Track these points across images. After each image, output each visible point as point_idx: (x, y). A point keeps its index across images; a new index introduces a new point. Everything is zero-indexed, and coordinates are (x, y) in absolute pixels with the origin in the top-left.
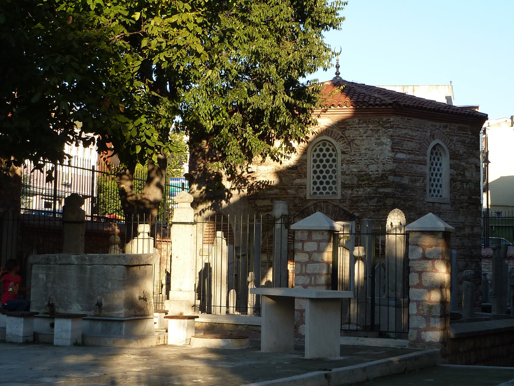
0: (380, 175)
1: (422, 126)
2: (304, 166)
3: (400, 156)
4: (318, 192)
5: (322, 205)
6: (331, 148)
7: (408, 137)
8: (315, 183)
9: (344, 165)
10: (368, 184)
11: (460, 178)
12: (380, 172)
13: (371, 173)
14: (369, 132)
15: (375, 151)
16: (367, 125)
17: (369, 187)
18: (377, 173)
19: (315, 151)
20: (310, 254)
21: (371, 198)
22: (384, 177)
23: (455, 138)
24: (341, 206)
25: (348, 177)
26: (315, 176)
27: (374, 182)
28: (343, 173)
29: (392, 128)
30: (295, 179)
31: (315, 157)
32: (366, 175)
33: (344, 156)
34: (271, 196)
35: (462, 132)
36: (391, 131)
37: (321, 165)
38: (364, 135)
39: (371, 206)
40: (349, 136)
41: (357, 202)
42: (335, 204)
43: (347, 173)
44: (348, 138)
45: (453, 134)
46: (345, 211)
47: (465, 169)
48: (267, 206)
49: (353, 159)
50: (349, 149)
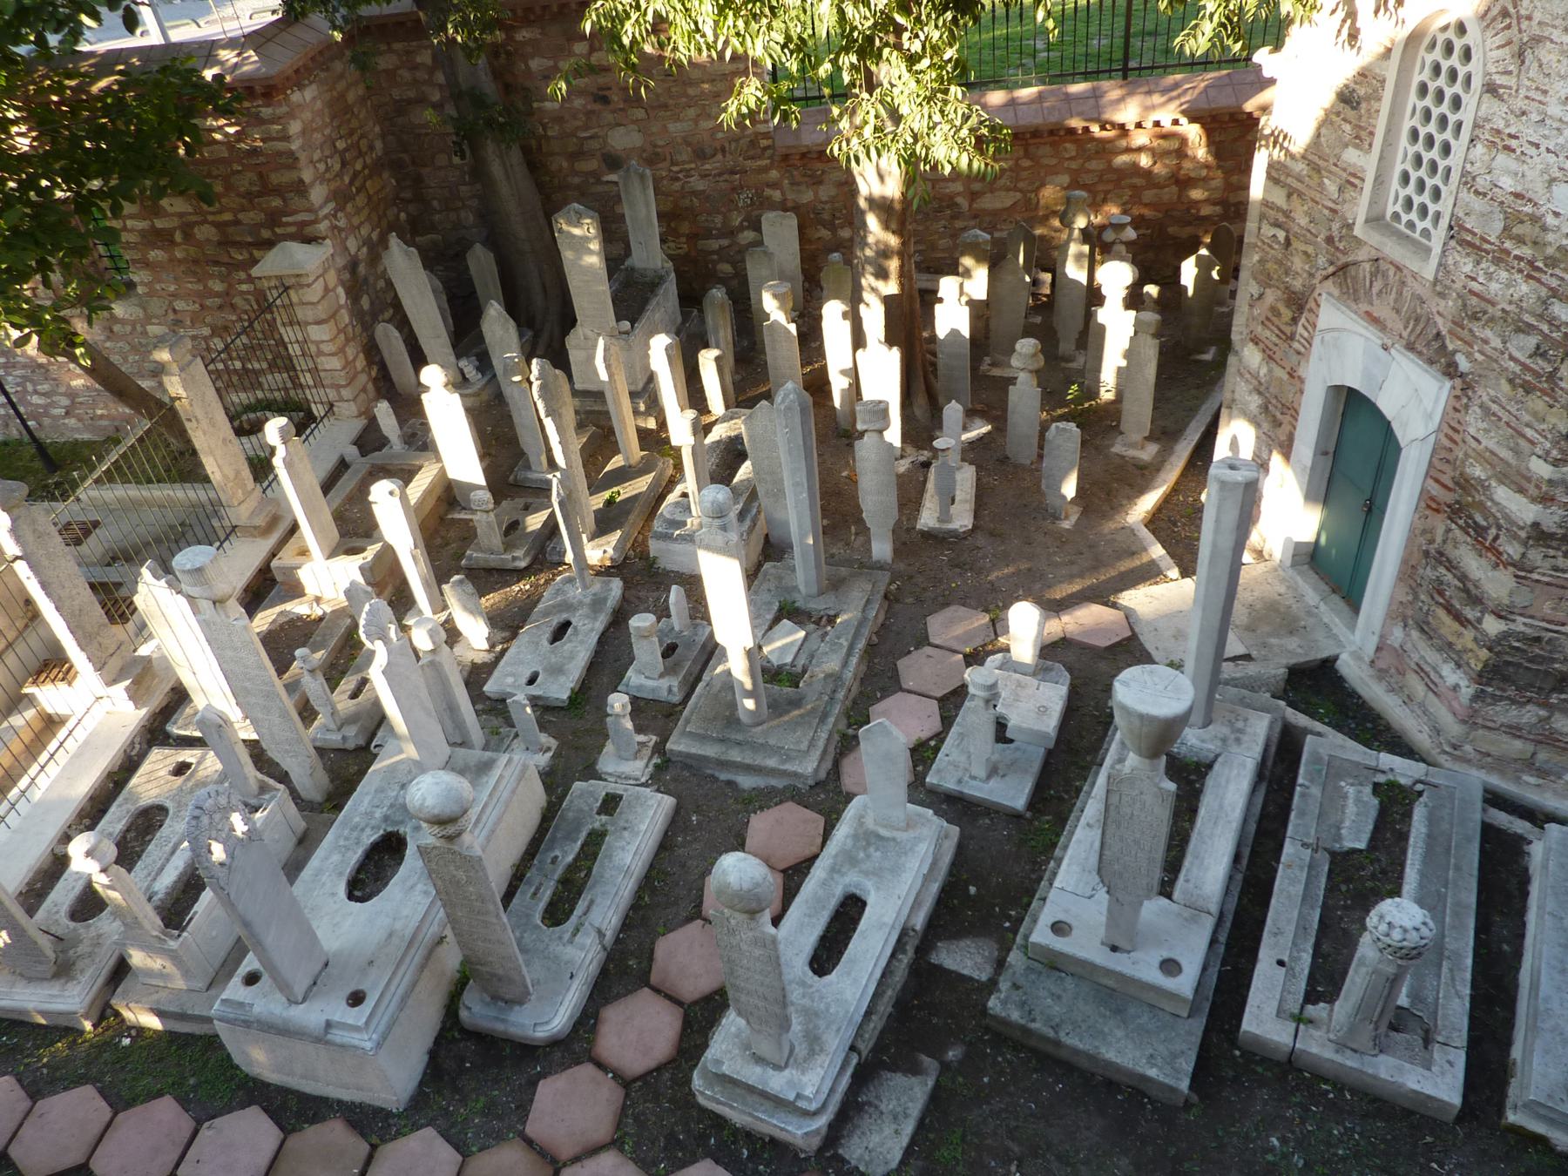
9: (1480, 149)
10: (1531, 263)
13: (1550, 220)
17: (1529, 277)
21: (1525, 329)
25: (1478, 204)
28: (1468, 180)
39: (1512, 358)
41: (1475, 317)
43: (1481, 183)
49: (1512, 130)
50: (1512, 82)
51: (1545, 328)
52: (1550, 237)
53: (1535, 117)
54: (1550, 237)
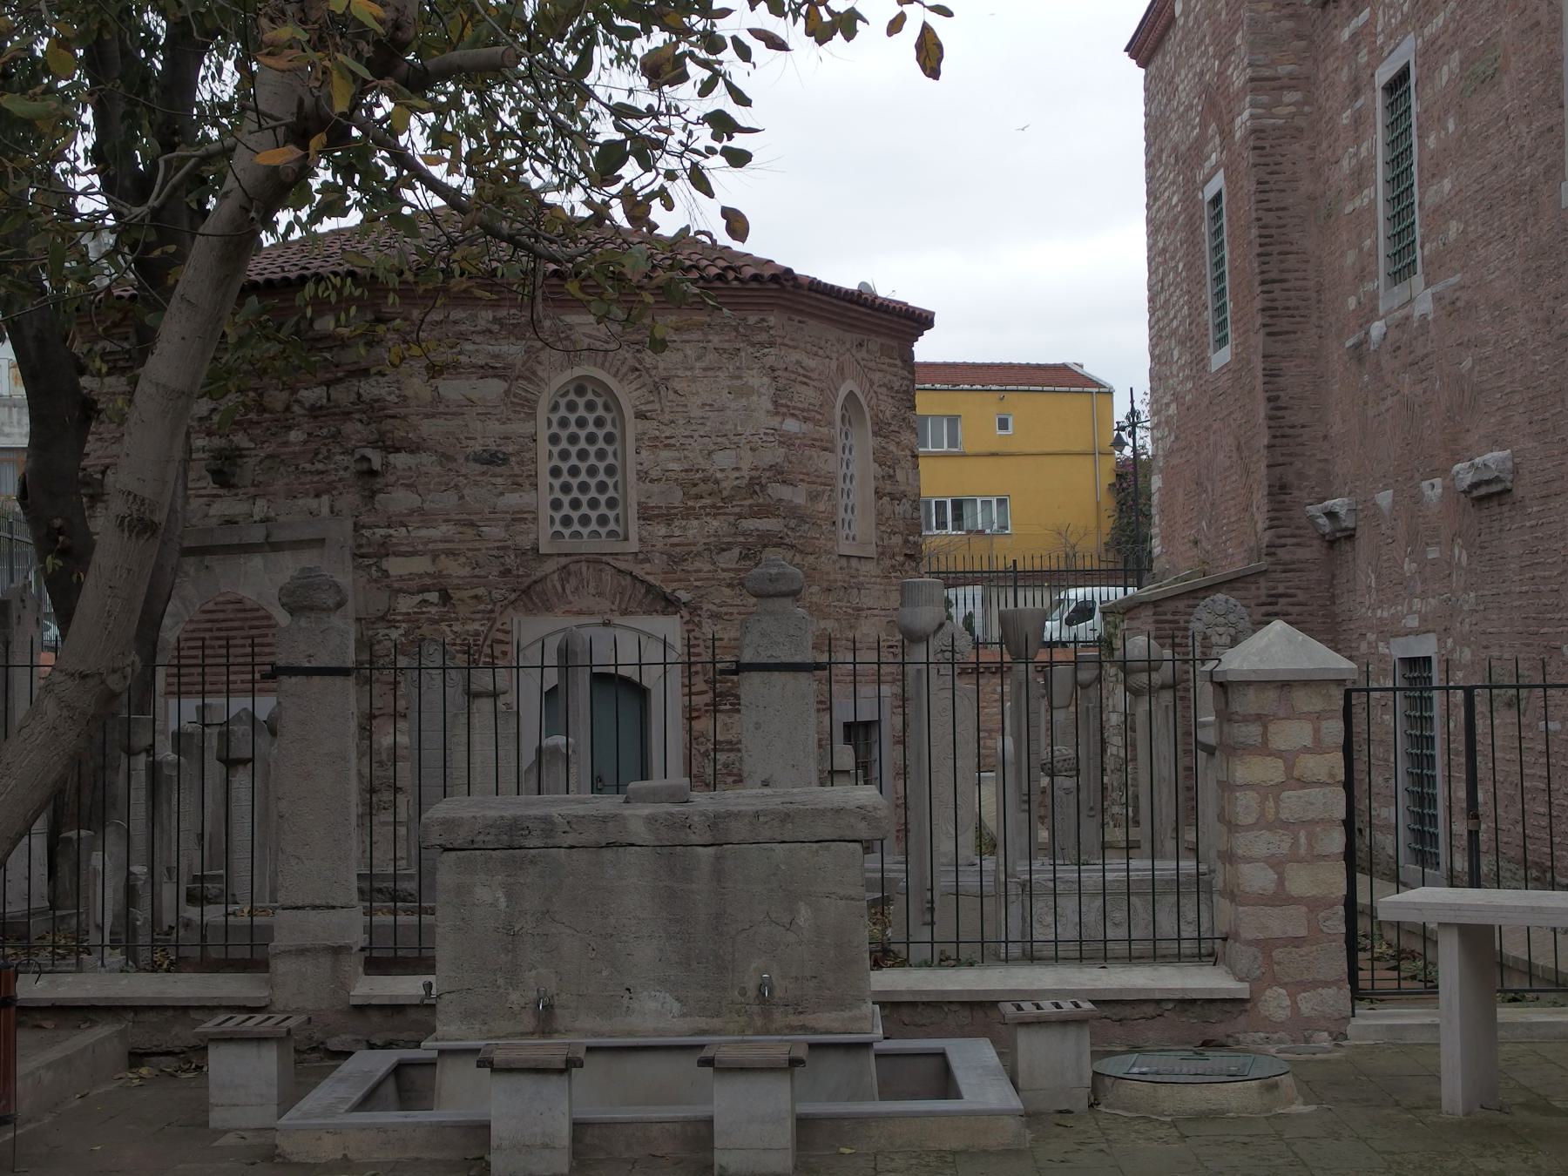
0: (745, 481)
1: (823, 343)
2: (528, 455)
3: (791, 425)
4: (567, 532)
5: (584, 569)
6: (600, 402)
7: (801, 371)
8: (556, 505)
9: (644, 453)
10: (713, 506)
11: (888, 488)
12: (745, 473)
13: (719, 475)
14: (711, 357)
15: (729, 413)
16: (705, 334)
18: (737, 474)
19: (555, 408)
21: (726, 548)
22: (757, 488)
23: (877, 376)
24: (638, 570)
25: (655, 487)
26: (557, 483)
27: (731, 498)
28: (643, 476)
29: (772, 345)
30: (502, 494)
31: (555, 429)
32: (705, 480)
33: (642, 425)
34: (431, 546)
35: (887, 360)
36: (772, 357)
37: (574, 450)
38: (698, 365)
39: (724, 570)
40: (656, 368)
42: (622, 566)
43: (654, 474)
44: (654, 372)
45: (872, 365)
46: (650, 588)
47: (897, 461)
48: (420, 576)
50: (657, 406)
51: (742, 539)
52: (724, 484)
53: (681, 421)
54: (724, 484)
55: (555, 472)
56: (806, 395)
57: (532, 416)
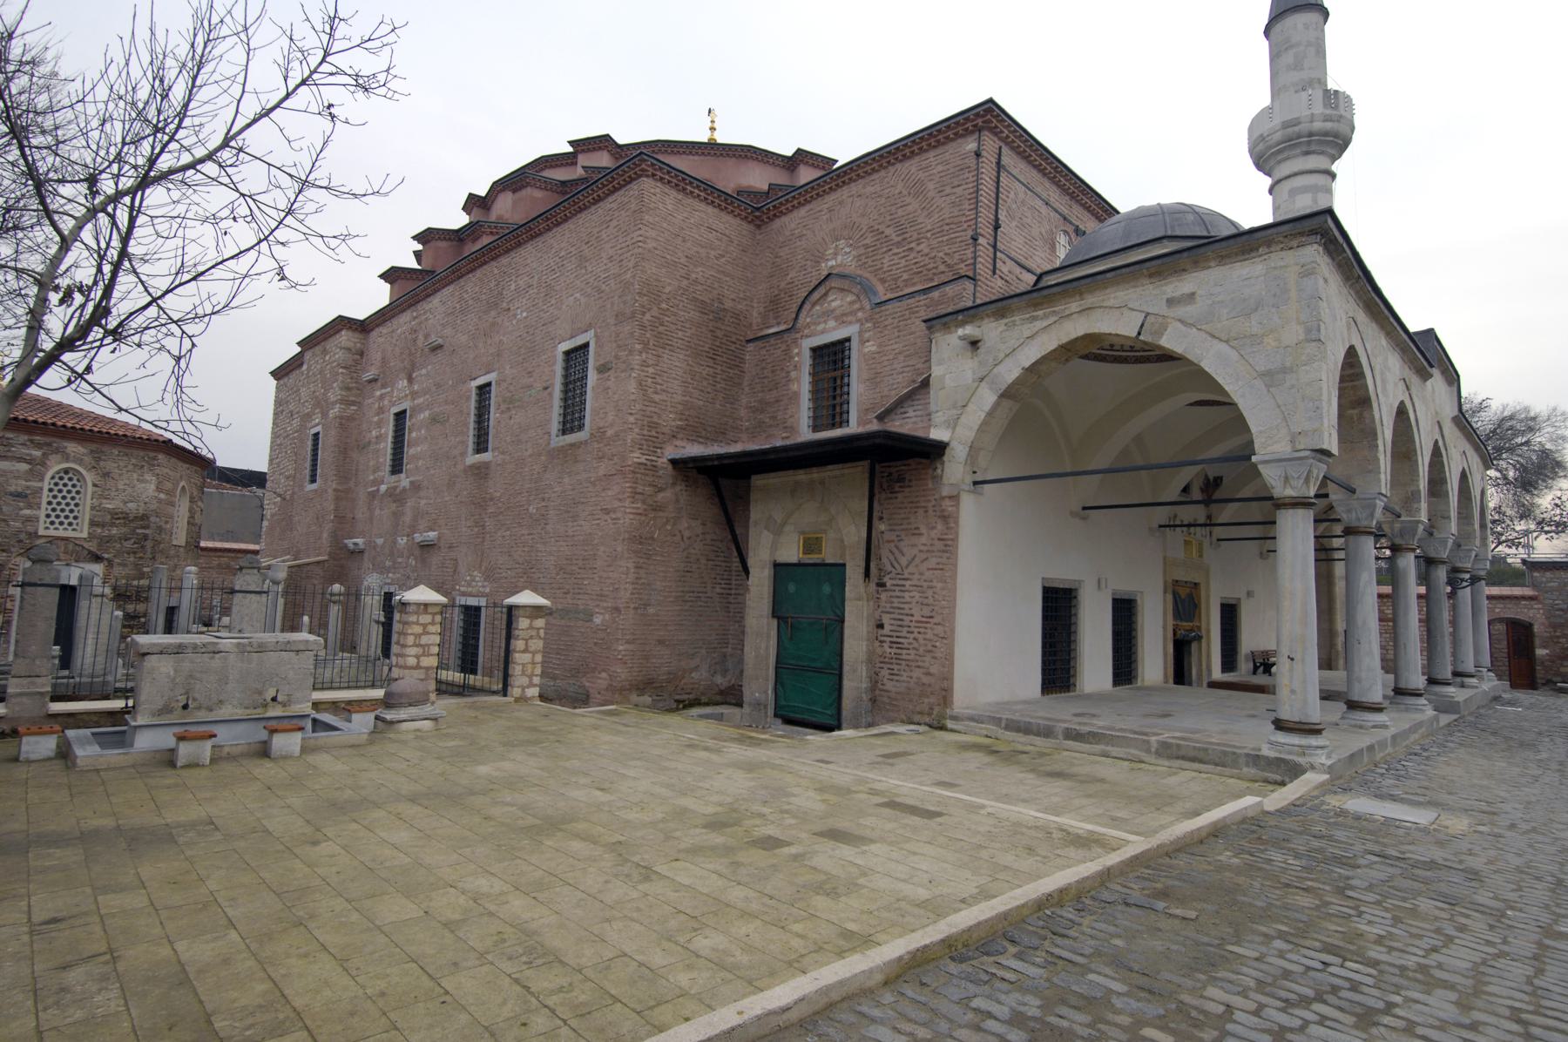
3: (162, 496)
8: (48, 516)
20: (425, 626)
24: (86, 545)
28: (93, 508)
46: (90, 552)
55: (50, 503)
56: (168, 485)
57: (42, 480)
